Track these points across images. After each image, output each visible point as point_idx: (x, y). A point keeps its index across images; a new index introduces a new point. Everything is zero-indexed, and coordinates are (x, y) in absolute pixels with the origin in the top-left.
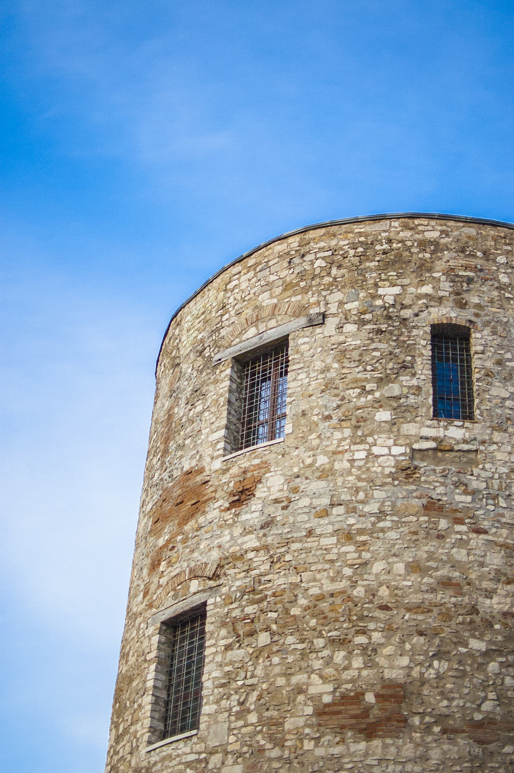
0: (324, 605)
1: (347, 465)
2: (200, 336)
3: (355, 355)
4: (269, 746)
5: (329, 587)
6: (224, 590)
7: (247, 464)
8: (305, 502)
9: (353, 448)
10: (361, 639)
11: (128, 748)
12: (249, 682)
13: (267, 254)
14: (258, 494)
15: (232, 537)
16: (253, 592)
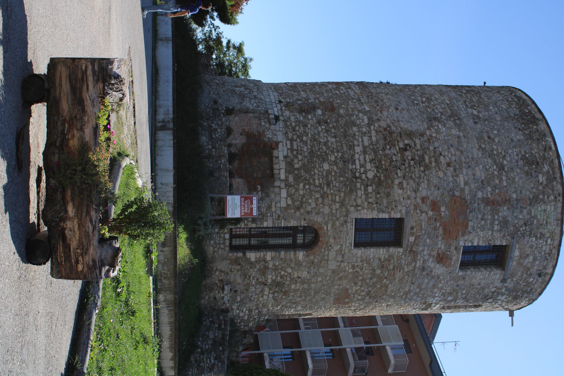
0: (384, 289)
1: (435, 292)
2: (535, 222)
3: (481, 291)
4: (339, 276)
5: (389, 290)
6: (403, 257)
8: (426, 281)
9: (441, 293)
10: (368, 297)
11: (359, 201)
12: (364, 268)
14: (438, 266)
15: (424, 255)
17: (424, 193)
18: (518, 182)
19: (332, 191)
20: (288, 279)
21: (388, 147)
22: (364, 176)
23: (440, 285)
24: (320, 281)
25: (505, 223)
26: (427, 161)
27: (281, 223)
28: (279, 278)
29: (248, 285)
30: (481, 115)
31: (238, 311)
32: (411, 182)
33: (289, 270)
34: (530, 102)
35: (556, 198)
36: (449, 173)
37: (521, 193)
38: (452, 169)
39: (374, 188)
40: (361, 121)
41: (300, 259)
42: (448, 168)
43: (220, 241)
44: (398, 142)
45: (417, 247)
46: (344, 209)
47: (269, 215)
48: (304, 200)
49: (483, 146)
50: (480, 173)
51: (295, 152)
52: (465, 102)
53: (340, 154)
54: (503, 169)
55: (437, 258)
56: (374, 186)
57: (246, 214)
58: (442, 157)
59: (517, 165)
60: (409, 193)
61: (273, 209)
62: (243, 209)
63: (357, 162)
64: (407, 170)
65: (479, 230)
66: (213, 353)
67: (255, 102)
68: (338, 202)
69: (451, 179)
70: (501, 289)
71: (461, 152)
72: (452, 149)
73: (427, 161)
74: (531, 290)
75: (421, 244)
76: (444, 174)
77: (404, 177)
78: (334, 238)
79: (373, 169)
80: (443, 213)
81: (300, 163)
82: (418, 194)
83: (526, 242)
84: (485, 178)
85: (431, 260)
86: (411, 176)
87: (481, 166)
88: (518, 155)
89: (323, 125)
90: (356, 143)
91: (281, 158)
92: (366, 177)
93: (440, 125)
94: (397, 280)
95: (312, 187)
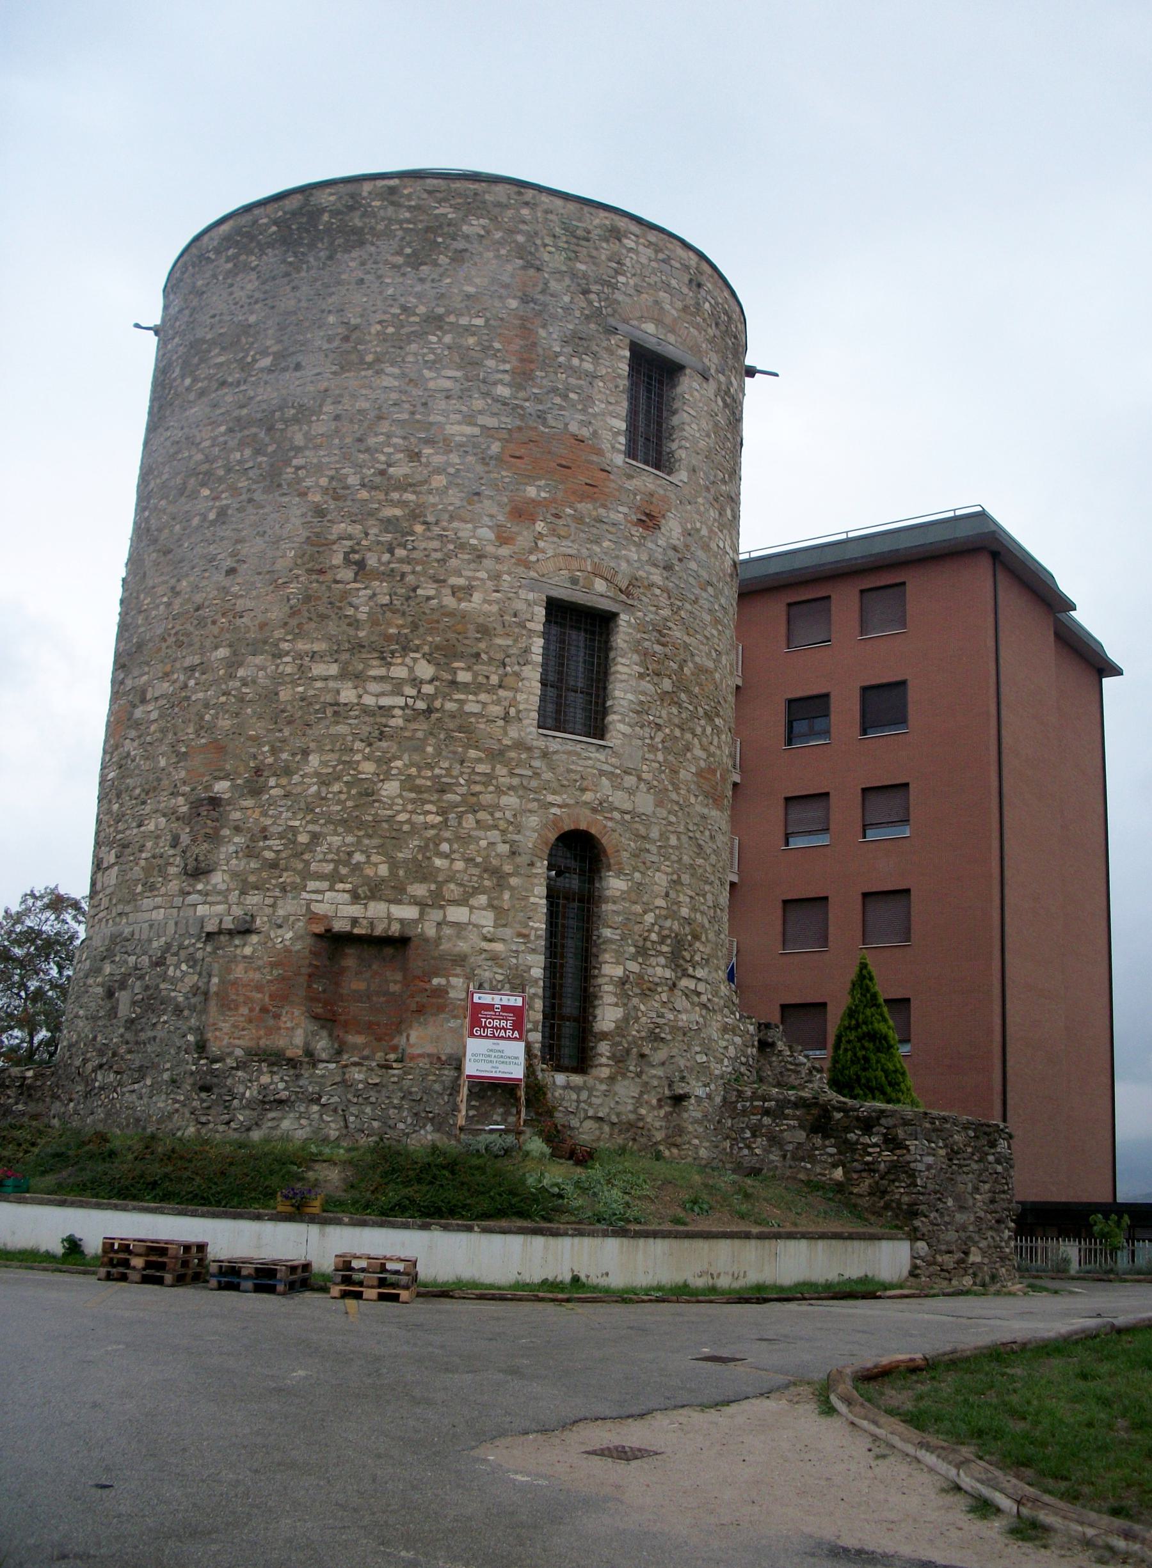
4: (670, 788)
7: (651, 487)
11: (496, 710)
12: (658, 721)
13: (669, 246)
15: (639, 560)
16: (660, 632)
17: (486, 533)
18: (477, 287)
19: (462, 781)
20: (668, 923)
21: (350, 612)
22: (428, 689)
23: (704, 532)
24: (679, 839)
25: (577, 342)
26: (398, 512)
27: (537, 929)
28: (665, 949)
29: (675, 1029)
30: (275, 349)
31: (726, 1062)
32: (453, 562)
33: (649, 918)
34: (246, 219)
35: (527, 204)
36: (438, 460)
37: (506, 286)
38: (427, 451)
39: (462, 665)
40: (261, 673)
41: (626, 888)
42: (424, 460)
43: (570, 1100)
44: (337, 582)
45: (620, 577)
46: (513, 754)
47: (514, 961)
48: (479, 860)
49: (369, 358)
50: (445, 379)
51: (344, 871)
52: (223, 384)
53: (358, 745)
54: (440, 318)
55: (647, 528)
56: (456, 665)
57: (518, 1026)
58: (391, 470)
59: (433, 281)
60: (483, 575)
61: (498, 947)
62: (502, 1033)
63: (385, 701)
64: (419, 568)
65: (590, 410)
66: (851, 1136)
67: (178, 966)
68: (493, 769)
69: (454, 458)
70: (719, 383)
71: (380, 418)
72: (372, 441)
73: (398, 512)
74: (726, 313)
75: (612, 565)
76: (439, 474)
77: (437, 581)
78: (583, 790)
79: (408, 660)
80: (543, 495)
81: (375, 858)
82: (490, 549)
83: (628, 299)
84: (460, 368)
85: (650, 545)
86: (438, 561)
87: (427, 373)
88: (404, 275)
89: (267, 781)
90: (329, 698)
91: (355, 910)
92: (431, 681)
93: (295, 462)
94: (686, 638)
95: (447, 834)
